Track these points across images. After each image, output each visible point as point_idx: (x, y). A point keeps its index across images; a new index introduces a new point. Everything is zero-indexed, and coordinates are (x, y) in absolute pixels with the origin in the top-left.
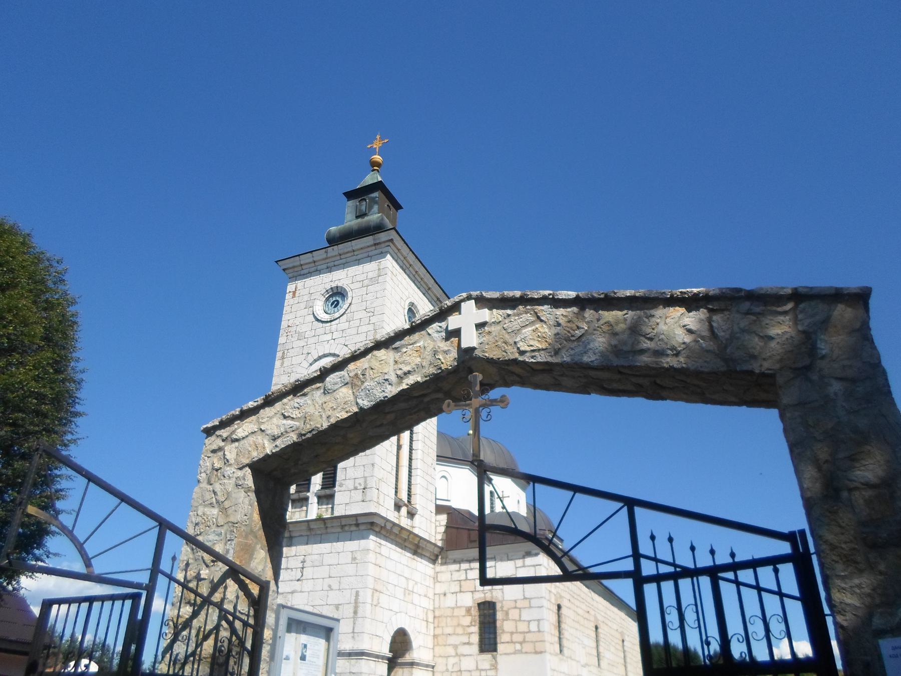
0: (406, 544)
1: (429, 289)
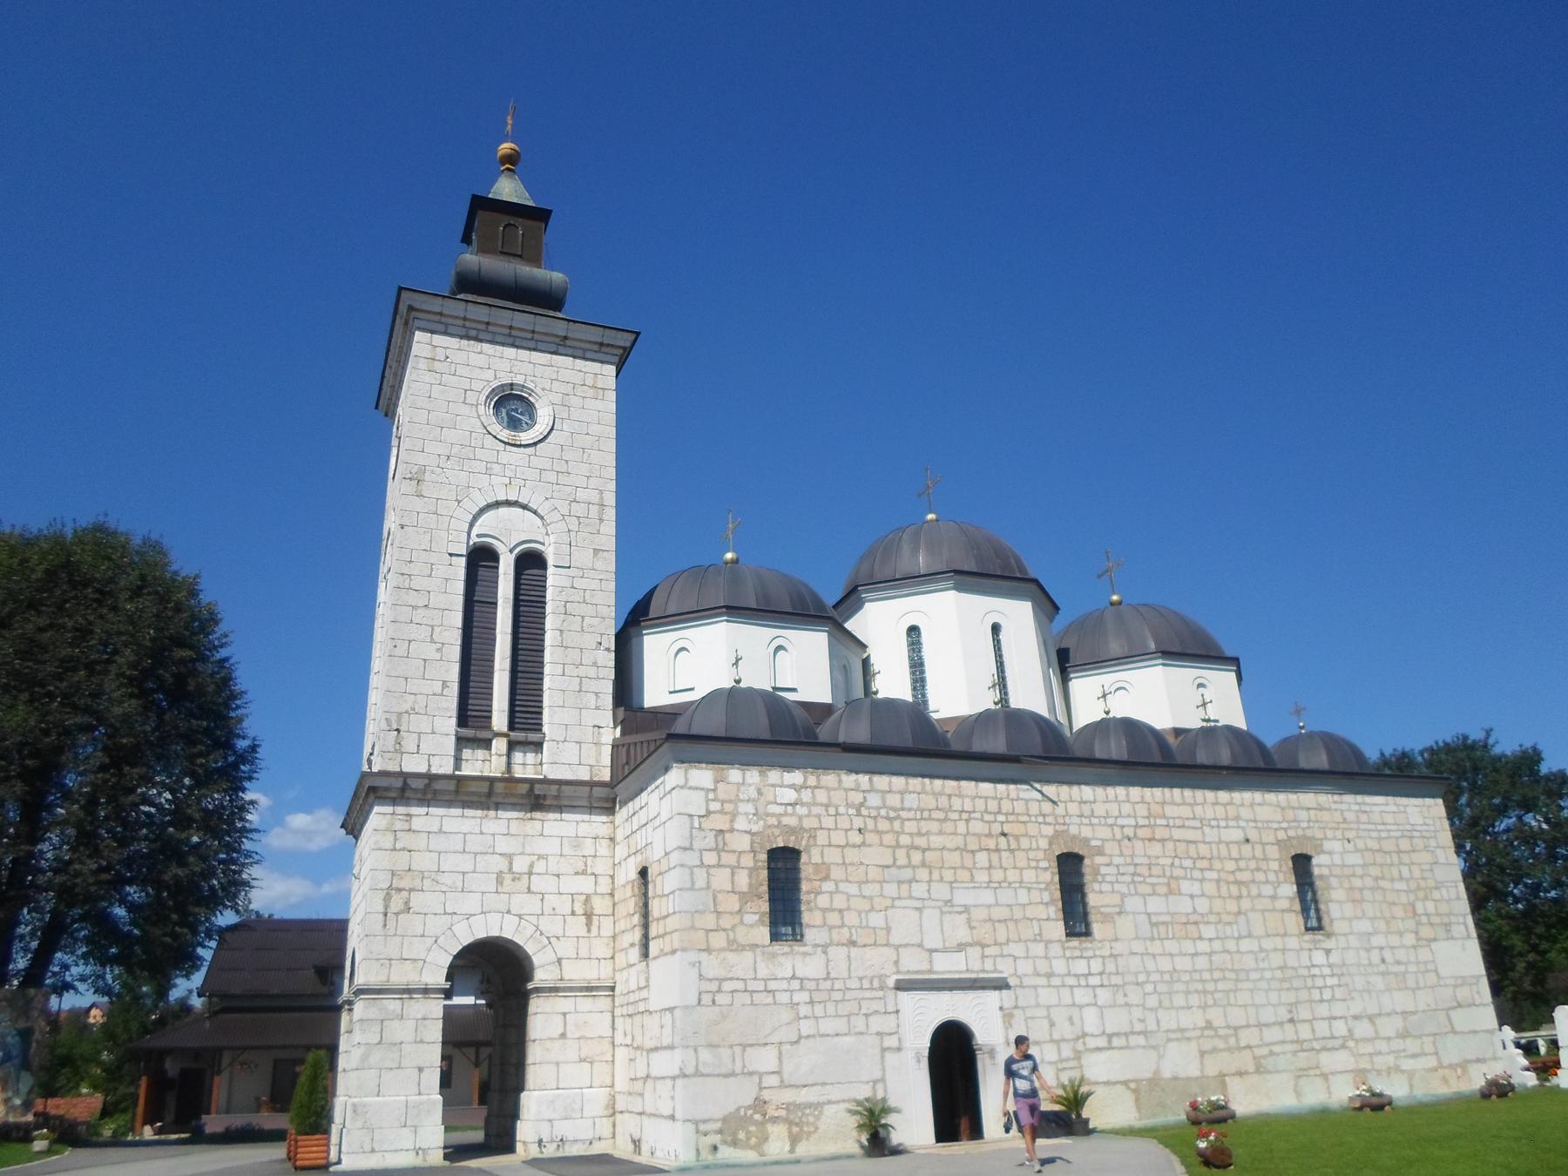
0: (494, 799)
1: (566, 338)
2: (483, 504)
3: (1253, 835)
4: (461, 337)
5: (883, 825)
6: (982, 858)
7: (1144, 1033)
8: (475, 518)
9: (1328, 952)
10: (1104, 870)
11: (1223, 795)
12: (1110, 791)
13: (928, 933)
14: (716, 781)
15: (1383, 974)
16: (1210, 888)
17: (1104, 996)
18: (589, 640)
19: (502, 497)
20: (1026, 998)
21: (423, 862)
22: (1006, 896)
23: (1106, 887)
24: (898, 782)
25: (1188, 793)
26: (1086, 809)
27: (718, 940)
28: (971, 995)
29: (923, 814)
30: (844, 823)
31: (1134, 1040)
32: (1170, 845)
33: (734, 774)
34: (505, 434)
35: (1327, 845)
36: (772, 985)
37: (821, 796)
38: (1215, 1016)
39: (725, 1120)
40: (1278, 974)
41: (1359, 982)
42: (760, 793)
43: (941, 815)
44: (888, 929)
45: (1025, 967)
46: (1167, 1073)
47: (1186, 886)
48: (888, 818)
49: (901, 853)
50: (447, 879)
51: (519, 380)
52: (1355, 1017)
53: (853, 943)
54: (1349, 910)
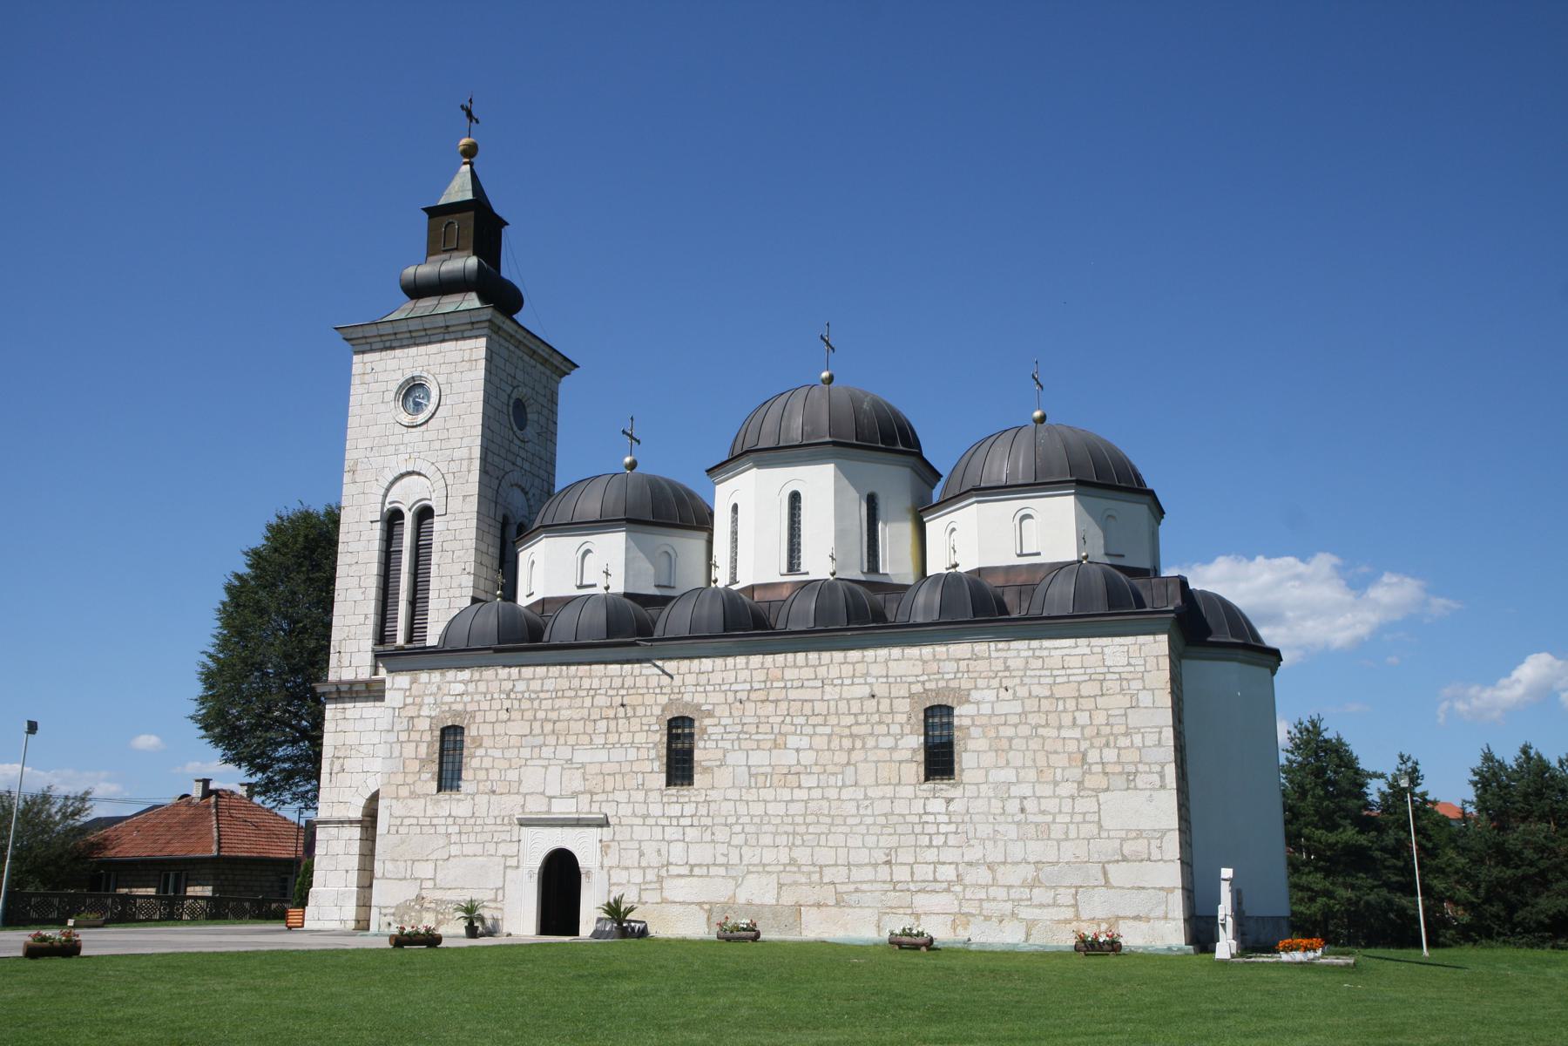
2: (391, 478)
3: (880, 690)
4: (381, 350)
5: (526, 704)
6: (602, 725)
7: (726, 866)
8: (388, 490)
9: (949, 801)
10: (710, 730)
11: (854, 655)
12: (730, 661)
13: (549, 784)
14: (412, 683)
15: (1018, 823)
16: (821, 742)
17: (692, 834)
18: (457, 568)
19: (403, 470)
20: (622, 833)
21: (351, 739)
22: (618, 754)
23: (710, 744)
24: (541, 670)
25: (813, 656)
26: (703, 679)
27: (404, 791)
28: (578, 830)
29: (558, 694)
30: (496, 705)
31: (713, 870)
32: (783, 706)
33: (424, 677)
34: (406, 419)
35: (975, 695)
36: (435, 821)
37: (482, 687)
38: (802, 855)
39: (397, 907)
40: (882, 820)
41: (984, 830)
42: (439, 688)
43: (573, 693)
44: (520, 782)
45: (625, 810)
46: (741, 899)
47: (793, 741)
48: (530, 699)
49: (536, 725)
50: (364, 749)
51: (416, 374)
52: (970, 864)
53: (494, 792)
54: (988, 759)
